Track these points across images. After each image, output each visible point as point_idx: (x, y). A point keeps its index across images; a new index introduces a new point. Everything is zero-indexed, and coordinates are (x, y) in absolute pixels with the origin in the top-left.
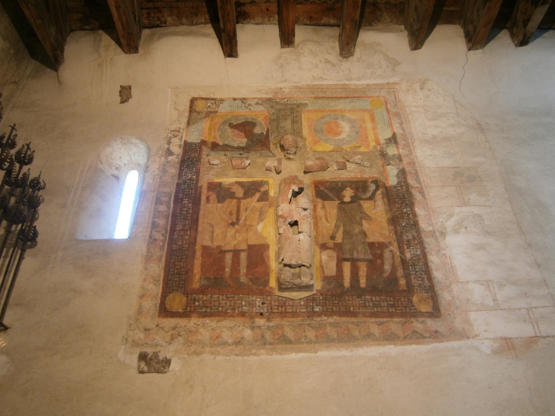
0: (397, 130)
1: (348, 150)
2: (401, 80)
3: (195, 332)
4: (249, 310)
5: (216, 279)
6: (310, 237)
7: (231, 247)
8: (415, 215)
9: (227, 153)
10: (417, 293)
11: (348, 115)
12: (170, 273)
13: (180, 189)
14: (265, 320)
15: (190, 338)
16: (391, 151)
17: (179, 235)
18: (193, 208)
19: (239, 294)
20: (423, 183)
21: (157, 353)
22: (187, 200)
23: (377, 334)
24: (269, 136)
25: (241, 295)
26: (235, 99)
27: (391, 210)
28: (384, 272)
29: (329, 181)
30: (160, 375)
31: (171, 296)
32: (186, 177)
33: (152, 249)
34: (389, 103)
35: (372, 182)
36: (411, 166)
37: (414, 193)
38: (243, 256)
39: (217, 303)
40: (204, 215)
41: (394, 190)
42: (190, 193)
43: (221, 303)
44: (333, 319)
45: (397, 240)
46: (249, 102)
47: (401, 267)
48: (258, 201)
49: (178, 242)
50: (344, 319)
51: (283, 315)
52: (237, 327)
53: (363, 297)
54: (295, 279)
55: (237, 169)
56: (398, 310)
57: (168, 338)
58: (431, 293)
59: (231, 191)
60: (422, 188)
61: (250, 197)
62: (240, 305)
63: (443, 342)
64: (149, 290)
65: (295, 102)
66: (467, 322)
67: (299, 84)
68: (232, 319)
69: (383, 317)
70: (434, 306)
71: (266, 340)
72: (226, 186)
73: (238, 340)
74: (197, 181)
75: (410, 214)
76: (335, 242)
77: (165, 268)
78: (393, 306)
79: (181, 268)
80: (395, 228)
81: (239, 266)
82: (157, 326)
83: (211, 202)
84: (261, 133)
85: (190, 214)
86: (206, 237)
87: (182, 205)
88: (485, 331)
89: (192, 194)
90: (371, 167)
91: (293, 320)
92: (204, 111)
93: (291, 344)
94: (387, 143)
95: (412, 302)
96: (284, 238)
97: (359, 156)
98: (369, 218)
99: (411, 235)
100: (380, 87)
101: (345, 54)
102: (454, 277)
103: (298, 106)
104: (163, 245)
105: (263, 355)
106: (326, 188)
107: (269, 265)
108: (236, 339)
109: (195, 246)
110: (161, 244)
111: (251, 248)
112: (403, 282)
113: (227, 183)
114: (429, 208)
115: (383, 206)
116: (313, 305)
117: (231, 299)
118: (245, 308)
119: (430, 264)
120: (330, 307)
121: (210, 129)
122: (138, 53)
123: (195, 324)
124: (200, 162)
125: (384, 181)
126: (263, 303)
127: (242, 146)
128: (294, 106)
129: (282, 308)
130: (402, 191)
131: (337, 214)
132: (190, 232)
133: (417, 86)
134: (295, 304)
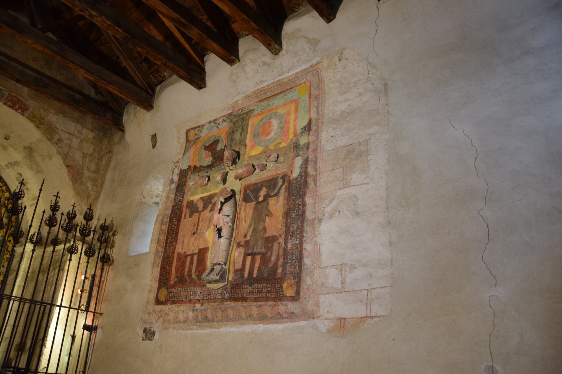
0: (314, 116)
2: (322, 58)
4: (194, 298)
7: (189, 253)
8: (304, 205)
9: (200, 174)
10: (288, 280)
14: (200, 305)
15: (165, 318)
16: (303, 141)
23: (255, 315)
25: (191, 288)
26: (210, 122)
27: (288, 203)
30: (150, 341)
31: (161, 290)
33: (156, 259)
35: (281, 178)
38: (195, 257)
39: (179, 294)
40: (181, 229)
45: (285, 233)
51: (209, 300)
52: (186, 310)
55: (202, 186)
62: (190, 295)
63: (295, 321)
66: (317, 304)
67: (247, 93)
68: (185, 305)
69: (261, 301)
70: (296, 291)
73: (185, 319)
75: (301, 204)
80: (287, 220)
82: (154, 310)
83: (186, 217)
88: (328, 312)
89: (178, 213)
91: (213, 304)
100: (306, 72)
101: (275, 52)
103: (247, 113)
104: (161, 255)
110: (160, 254)
111: (200, 250)
118: (191, 297)
122: (154, 108)
123: (169, 308)
126: (201, 293)
129: (209, 296)
133: (336, 59)
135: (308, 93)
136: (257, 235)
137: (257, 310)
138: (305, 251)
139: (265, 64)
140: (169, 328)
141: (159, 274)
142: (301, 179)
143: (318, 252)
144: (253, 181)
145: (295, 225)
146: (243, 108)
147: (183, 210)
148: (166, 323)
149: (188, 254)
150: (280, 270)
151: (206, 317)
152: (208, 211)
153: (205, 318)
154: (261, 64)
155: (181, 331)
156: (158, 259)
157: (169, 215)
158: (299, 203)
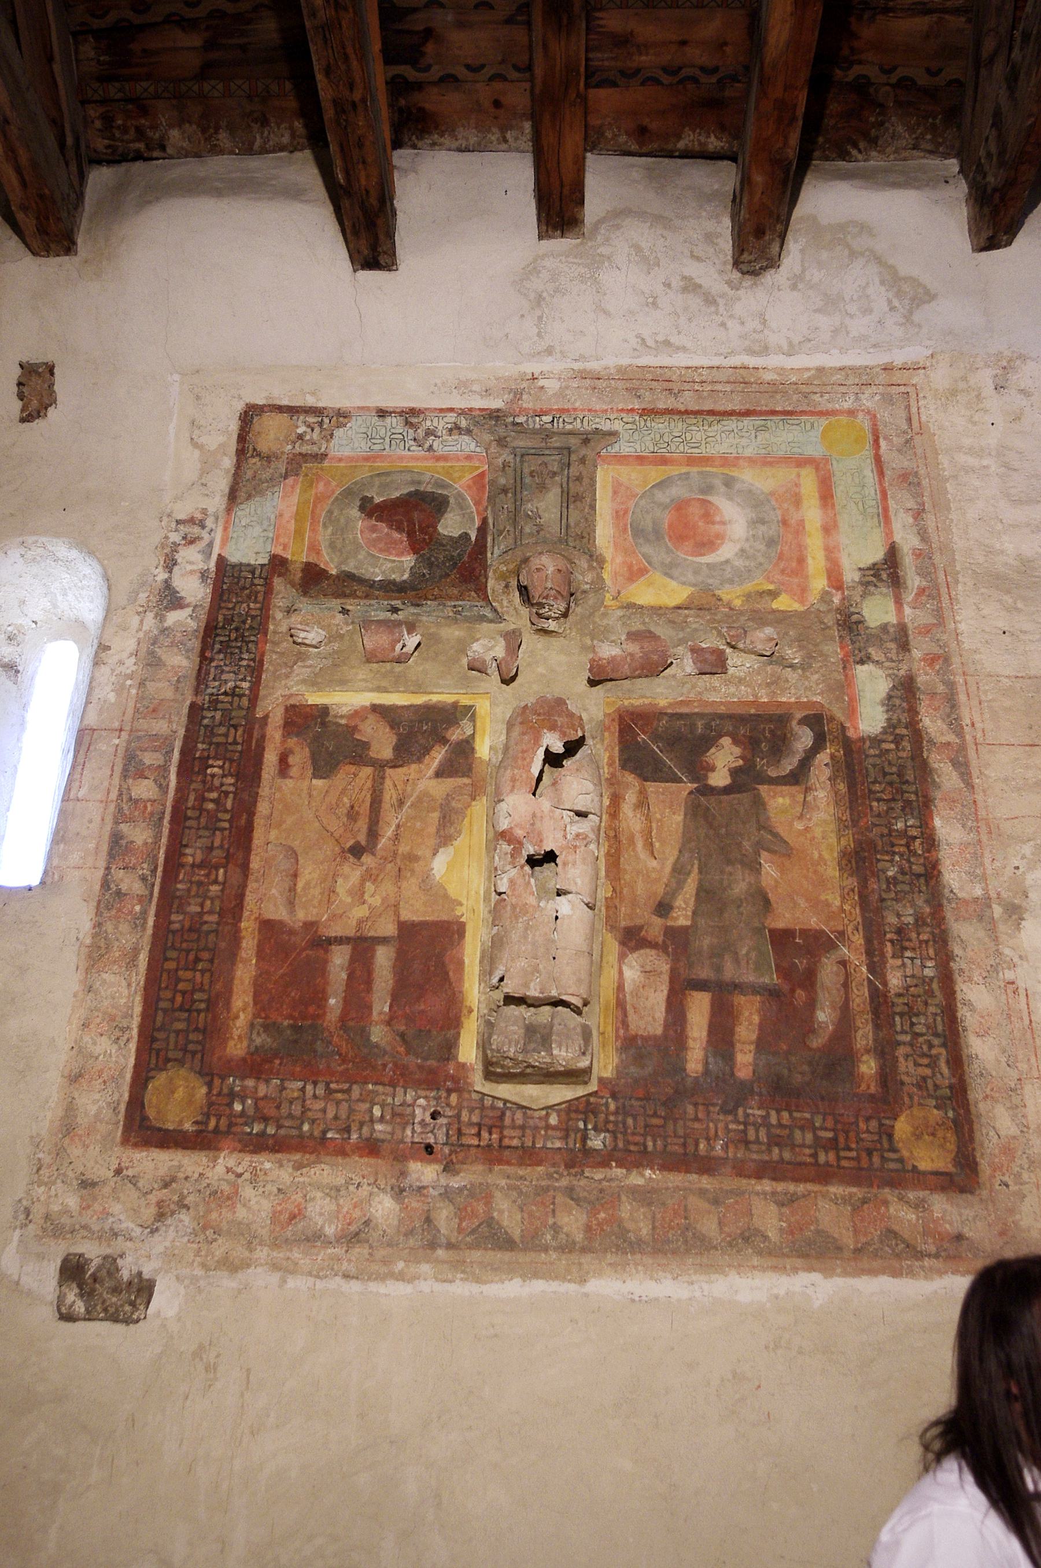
1: (737, 603)
2: (932, 355)
3: (228, 1198)
4: (393, 1134)
5: (295, 1028)
6: (591, 907)
8: (931, 842)
9: (351, 605)
10: (911, 1107)
11: (748, 477)
12: (163, 1005)
13: (201, 725)
14: (439, 1167)
15: (214, 1215)
17: (191, 882)
18: (235, 793)
19: (366, 1083)
20: (967, 729)
21: (115, 1260)
22: (220, 763)
24: (485, 547)
25: (370, 1086)
26: (382, 413)
27: (855, 823)
28: (812, 1031)
29: (666, 714)
30: (120, 1328)
31: (161, 1079)
32: (220, 685)
33: (109, 927)
34: (885, 438)
35: (805, 721)
36: (937, 667)
37: (936, 766)
38: (383, 958)
39: (296, 1109)
41: (872, 752)
42: (230, 740)
43: (309, 1110)
44: (643, 1176)
46: (428, 423)
47: (870, 1016)
48: (438, 774)
49: (189, 904)
50: (675, 1179)
52: (352, 1188)
53: (740, 1111)
54: (534, 1050)
55: (377, 662)
56: (846, 1158)
57: (149, 1213)
58: (953, 1109)
59: (357, 736)
60: (963, 748)
61: (414, 762)
64: (97, 1058)
65: (578, 424)
67: (593, 365)
68: (340, 1159)
69: (796, 1180)
70: (958, 1152)
71: (439, 1231)
72: (343, 722)
73: (353, 1228)
74: (254, 698)
75: (916, 838)
76: (670, 923)
77: (145, 989)
78: (833, 1145)
79: (193, 991)
80: (864, 884)
81: (369, 989)
82: (118, 1172)
83: (294, 771)
84: (460, 536)
85: (226, 811)
86: (274, 891)
87: (204, 782)
89: (235, 743)
90: (805, 666)
91: (521, 1172)
92: (283, 453)
93: (512, 1250)
94: (868, 583)
95: (890, 1136)
96: (509, 908)
97: (769, 631)
98: (782, 849)
99: (911, 912)
101: (750, 262)
102: (1033, 1060)
104: (144, 913)
105: (425, 1280)
106: (656, 737)
107: (461, 992)
108: (349, 1224)
109: (240, 920)
110: (138, 908)
111: (408, 931)
112: (868, 1067)
113: (344, 710)
114: (977, 820)
115: (831, 810)
116: (586, 1129)
117: (339, 1096)
118: (379, 1127)
119: (962, 1012)
120: (638, 1139)
121: (299, 517)
123: (229, 1170)
124: (266, 634)
125: (842, 719)
126: (434, 1116)
127: (398, 580)
128: (573, 441)
129: (490, 1134)
130: (900, 758)
131: (684, 826)
132: (226, 872)
133: (985, 378)
134: (531, 1122)
135: (868, 452)
136: (726, 915)
137: (781, 1214)
138: (965, 1008)
139: (690, 286)
140: (245, 1264)
141: (138, 999)
142: (897, 747)
143: (1027, 1022)
144: (662, 703)
145: (905, 906)
146: (563, 411)
147: (263, 737)
148: (220, 1241)
149: (336, 930)
150: (868, 1067)
151: (489, 1226)
152: (431, 772)
153: (484, 1229)
154: (676, 282)
155: (337, 1283)
156: (124, 927)
157: (178, 745)
158: (906, 831)
